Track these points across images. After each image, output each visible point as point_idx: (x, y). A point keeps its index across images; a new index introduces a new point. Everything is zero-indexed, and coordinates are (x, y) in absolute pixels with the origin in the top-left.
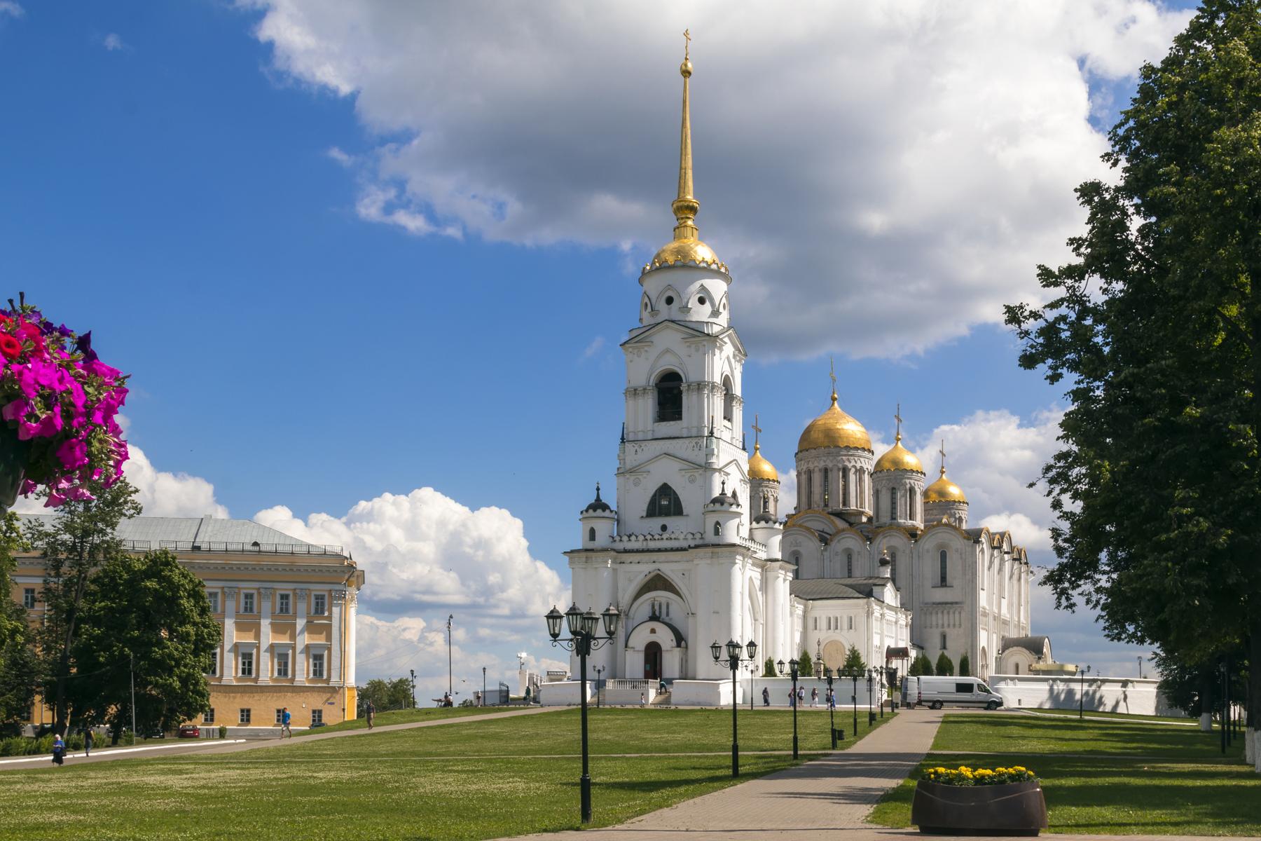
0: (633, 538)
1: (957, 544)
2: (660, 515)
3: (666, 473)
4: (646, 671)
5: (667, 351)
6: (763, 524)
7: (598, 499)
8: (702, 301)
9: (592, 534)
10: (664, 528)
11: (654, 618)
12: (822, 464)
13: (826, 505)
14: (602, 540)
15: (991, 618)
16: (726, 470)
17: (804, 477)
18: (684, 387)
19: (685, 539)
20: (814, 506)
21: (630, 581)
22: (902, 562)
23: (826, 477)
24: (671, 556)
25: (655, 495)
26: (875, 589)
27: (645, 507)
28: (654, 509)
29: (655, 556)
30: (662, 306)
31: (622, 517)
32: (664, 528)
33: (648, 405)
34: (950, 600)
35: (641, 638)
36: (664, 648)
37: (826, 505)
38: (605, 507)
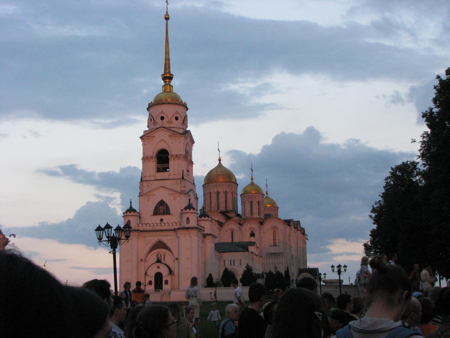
0: (148, 225)
1: (281, 226)
2: (160, 214)
3: (162, 195)
6: (203, 218)
7: (131, 207)
8: (177, 118)
10: (162, 220)
11: (159, 261)
12: (216, 190)
13: (218, 208)
15: (294, 260)
16: (189, 194)
17: (208, 197)
18: (170, 157)
20: (213, 209)
21: (147, 244)
22: (257, 234)
23: (218, 196)
24: (167, 233)
25: (157, 205)
26: (249, 247)
28: (156, 212)
29: (158, 233)
30: (159, 120)
31: (142, 216)
32: (162, 220)
33: (153, 164)
34: (277, 252)
36: (163, 275)
37: (218, 208)
38: (134, 211)
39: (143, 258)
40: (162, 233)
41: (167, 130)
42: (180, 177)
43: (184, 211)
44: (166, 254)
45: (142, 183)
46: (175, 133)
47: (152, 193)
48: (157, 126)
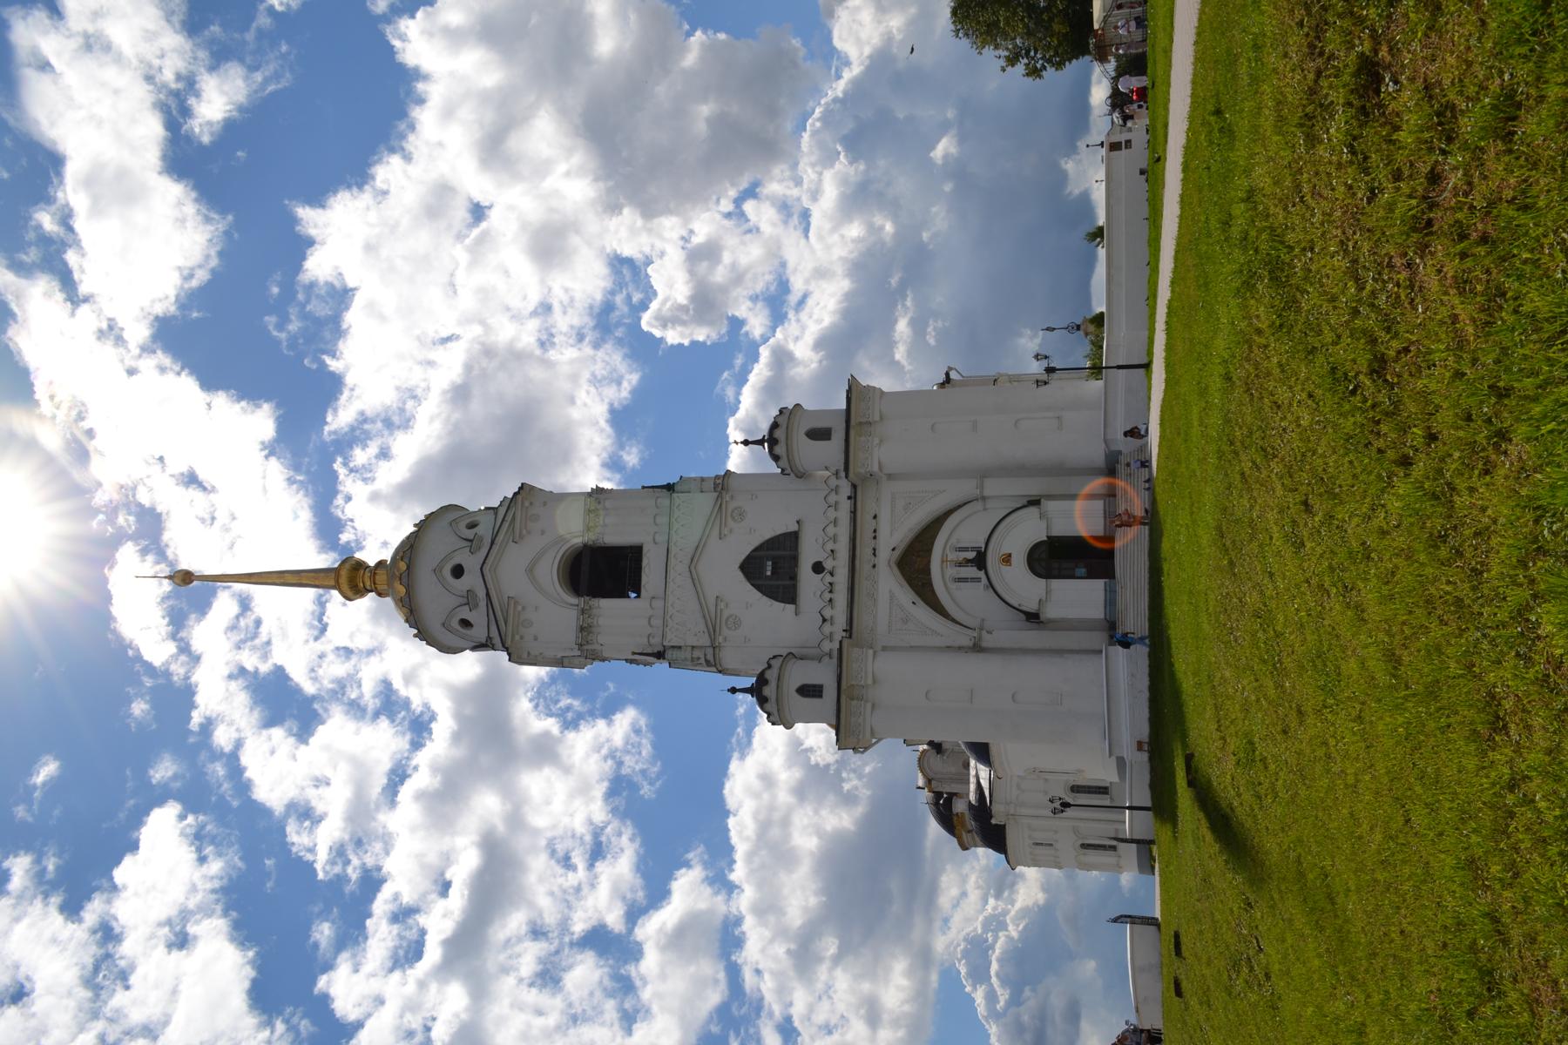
0: (828, 613)
2: (793, 577)
4: (1091, 575)
5: (530, 570)
8: (472, 526)
9: (810, 691)
10: (818, 568)
11: (980, 561)
14: (821, 674)
19: (836, 506)
21: (905, 621)
24: (866, 525)
25: (758, 588)
27: (779, 606)
32: (818, 568)
35: (1024, 586)
39: (966, 641)
40: (864, 552)
41: (496, 548)
42: (664, 499)
43: (779, 450)
44: (953, 541)
45: (669, 654)
46: (509, 518)
47: (713, 609)
48: (481, 594)
